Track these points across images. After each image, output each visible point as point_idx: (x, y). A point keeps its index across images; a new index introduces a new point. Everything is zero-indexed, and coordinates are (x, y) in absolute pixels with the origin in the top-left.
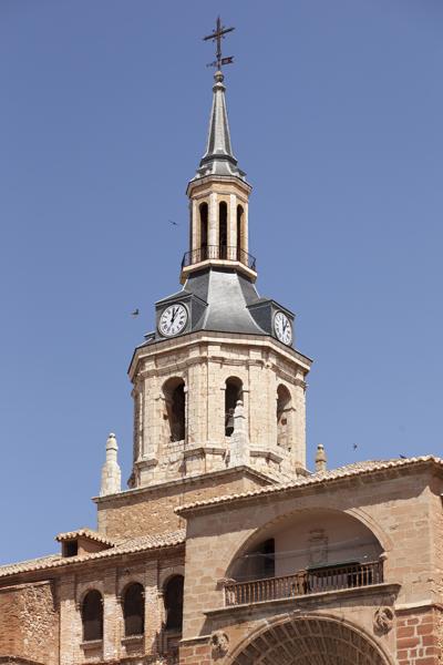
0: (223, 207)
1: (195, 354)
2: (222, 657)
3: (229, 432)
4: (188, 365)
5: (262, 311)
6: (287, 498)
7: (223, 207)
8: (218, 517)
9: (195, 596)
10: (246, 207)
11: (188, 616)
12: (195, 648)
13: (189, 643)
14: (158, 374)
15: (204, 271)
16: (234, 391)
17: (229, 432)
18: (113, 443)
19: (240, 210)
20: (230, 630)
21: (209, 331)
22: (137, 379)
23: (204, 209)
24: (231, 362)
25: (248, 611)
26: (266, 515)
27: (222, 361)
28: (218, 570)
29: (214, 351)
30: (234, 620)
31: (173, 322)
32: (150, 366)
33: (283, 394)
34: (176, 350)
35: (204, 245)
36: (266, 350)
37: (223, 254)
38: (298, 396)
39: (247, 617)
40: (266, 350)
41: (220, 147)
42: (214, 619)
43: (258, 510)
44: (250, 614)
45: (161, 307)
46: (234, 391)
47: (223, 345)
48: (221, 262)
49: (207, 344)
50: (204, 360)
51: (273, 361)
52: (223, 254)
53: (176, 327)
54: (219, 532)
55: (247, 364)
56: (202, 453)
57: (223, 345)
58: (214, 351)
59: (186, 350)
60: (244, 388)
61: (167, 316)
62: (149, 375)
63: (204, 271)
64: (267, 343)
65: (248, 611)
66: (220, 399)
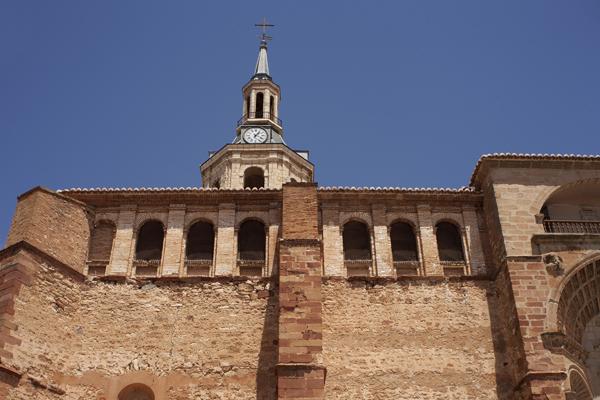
2: (559, 274)
4: (268, 162)
6: (588, 168)
8: (523, 172)
9: (512, 224)
10: (276, 98)
11: (509, 238)
12: (525, 264)
13: (518, 259)
14: (242, 163)
19: (272, 99)
20: (564, 255)
25: (580, 240)
26: (572, 177)
28: (532, 208)
30: (565, 246)
39: (578, 245)
42: (544, 243)
43: (561, 172)
44: (581, 243)
54: (526, 182)
58: (285, 159)
59: (267, 153)
62: (236, 161)
65: (580, 240)
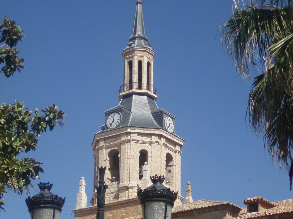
0: (140, 63)
1: (124, 138)
3: (141, 177)
5: (159, 117)
7: (140, 63)
10: (152, 63)
14: (107, 148)
15: (130, 95)
16: (143, 157)
17: (141, 177)
18: (83, 182)
19: (149, 64)
21: (131, 127)
22: (96, 150)
23: (131, 64)
24: (143, 142)
27: (138, 141)
29: (133, 137)
31: (115, 120)
32: (102, 144)
33: (169, 158)
34: (117, 136)
35: (131, 81)
36: (160, 136)
37: (140, 87)
38: (177, 159)
40: (160, 136)
41: (139, 32)
45: (108, 114)
46: (143, 157)
47: (139, 134)
48: (138, 91)
49: (130, 133)
50: (129, 141)
51: (163, 140)
52: (140, 87)
53: (115, 125)
55: (150, 143)
56: (127, 188)
57: (139, 134)
58: (133, 137)
59: (120, 136)
60: (149, 155)
61: (110, 119)
63: (130, 95)
64: (161, 132)
66: (136, 161)
